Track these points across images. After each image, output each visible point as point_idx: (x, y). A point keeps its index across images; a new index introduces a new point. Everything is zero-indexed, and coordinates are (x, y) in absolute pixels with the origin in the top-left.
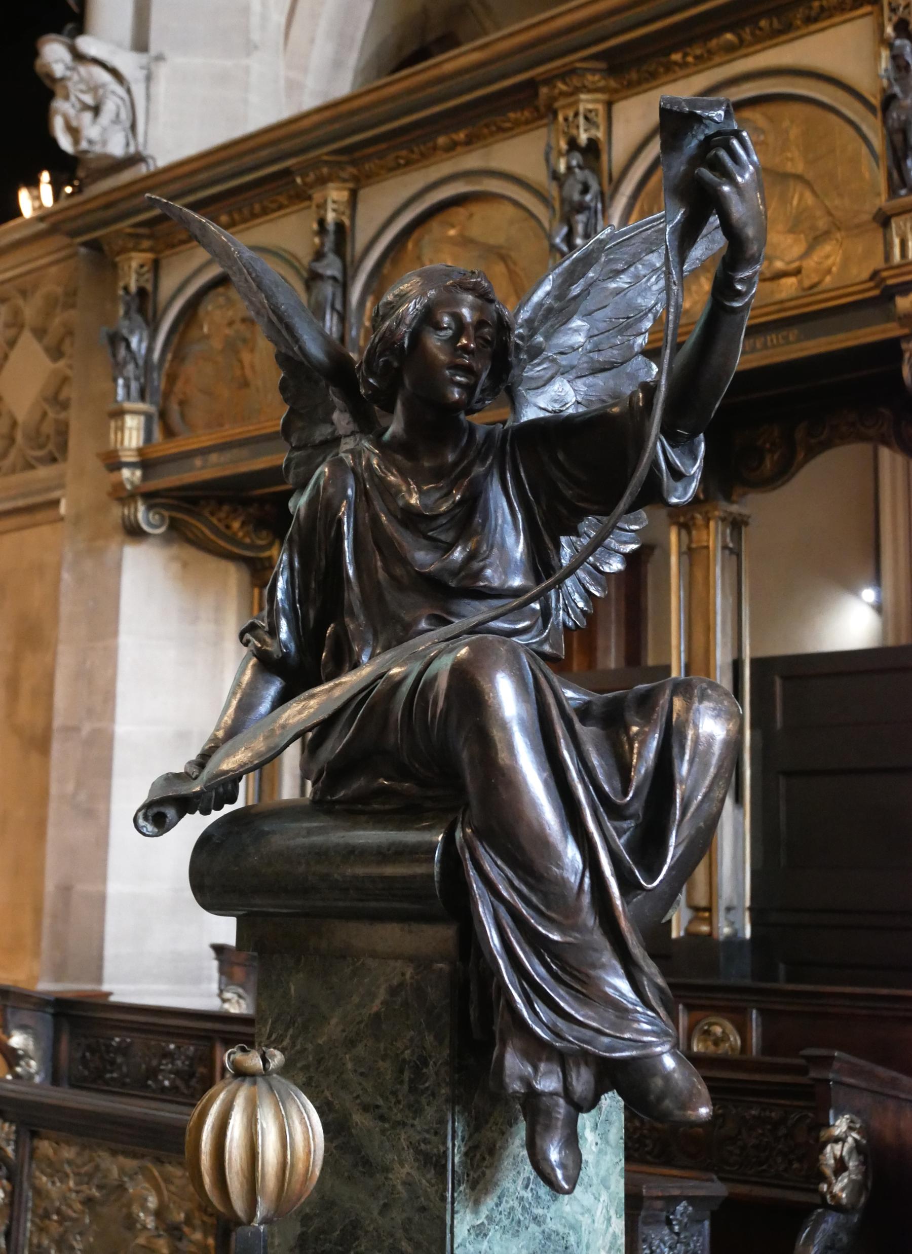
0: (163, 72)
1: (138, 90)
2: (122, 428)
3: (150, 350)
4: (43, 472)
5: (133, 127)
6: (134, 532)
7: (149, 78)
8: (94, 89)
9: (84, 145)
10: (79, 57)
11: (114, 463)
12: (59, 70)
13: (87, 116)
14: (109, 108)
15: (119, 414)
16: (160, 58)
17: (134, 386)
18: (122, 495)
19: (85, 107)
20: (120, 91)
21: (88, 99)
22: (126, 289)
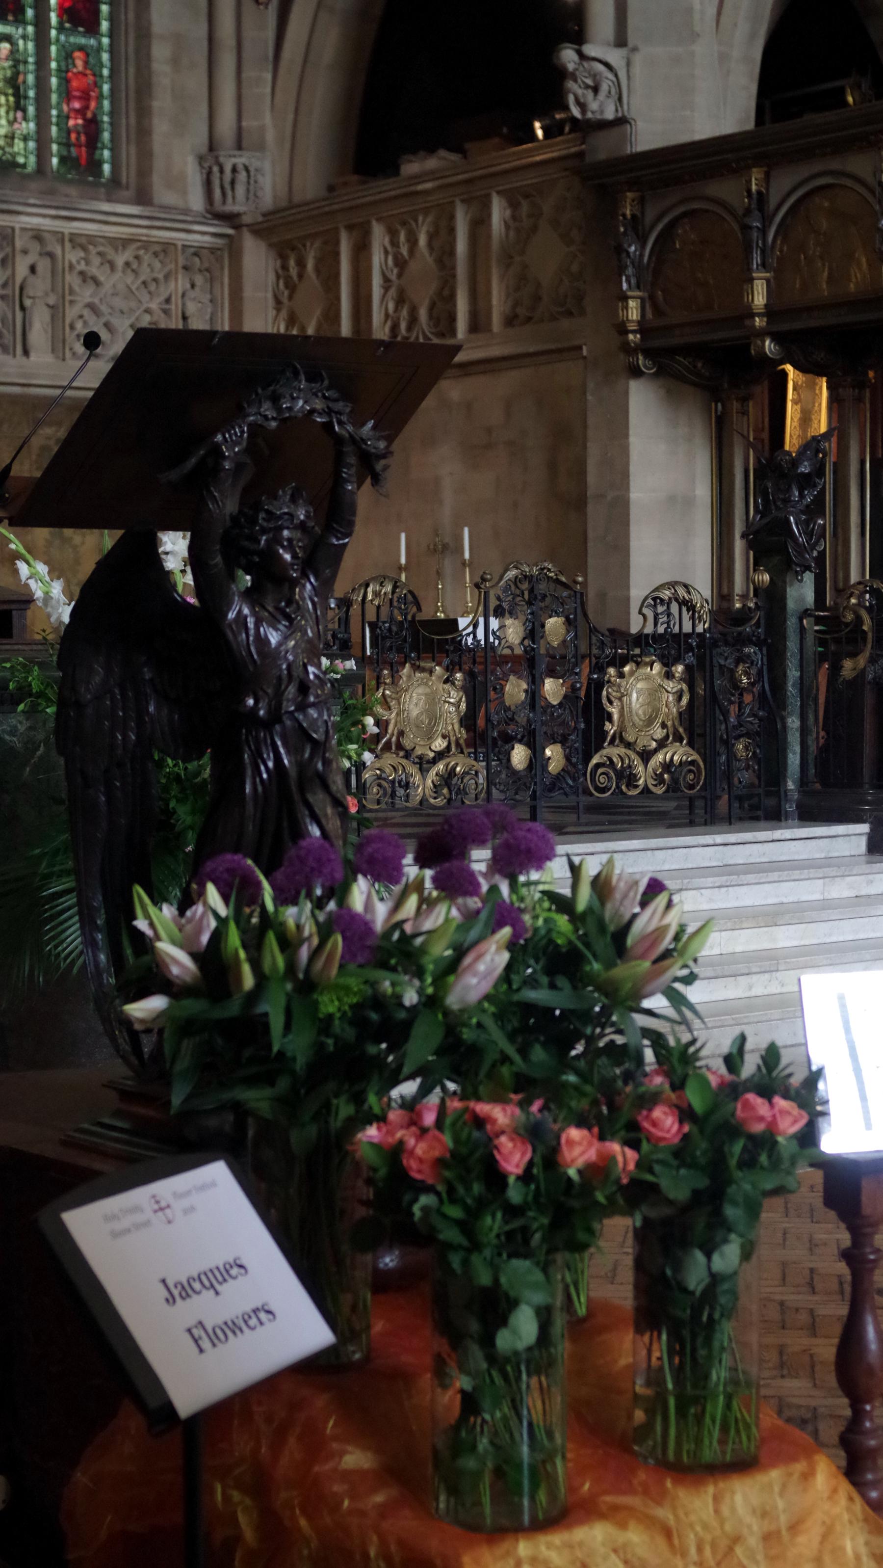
0: (637, 59)
1: (622, 75)
2: (627, 308)
3: (642, 255)
4: (565, 323)
5: (620, 99)
6: (636, 372)
7: (628, 64)
8: (595, 76)
9: (589, 115)
10: (582, 56)
11: (622, 329)
12: (571, 67)
13: (590, 94)
14: (604, 88)
15: (625, 298)
16: (635, 49)
17: (633, 281)
18: (627, 349)
19: (587, 87)
20: (611, 76)
21: (589, 82)
22: (624, 215)
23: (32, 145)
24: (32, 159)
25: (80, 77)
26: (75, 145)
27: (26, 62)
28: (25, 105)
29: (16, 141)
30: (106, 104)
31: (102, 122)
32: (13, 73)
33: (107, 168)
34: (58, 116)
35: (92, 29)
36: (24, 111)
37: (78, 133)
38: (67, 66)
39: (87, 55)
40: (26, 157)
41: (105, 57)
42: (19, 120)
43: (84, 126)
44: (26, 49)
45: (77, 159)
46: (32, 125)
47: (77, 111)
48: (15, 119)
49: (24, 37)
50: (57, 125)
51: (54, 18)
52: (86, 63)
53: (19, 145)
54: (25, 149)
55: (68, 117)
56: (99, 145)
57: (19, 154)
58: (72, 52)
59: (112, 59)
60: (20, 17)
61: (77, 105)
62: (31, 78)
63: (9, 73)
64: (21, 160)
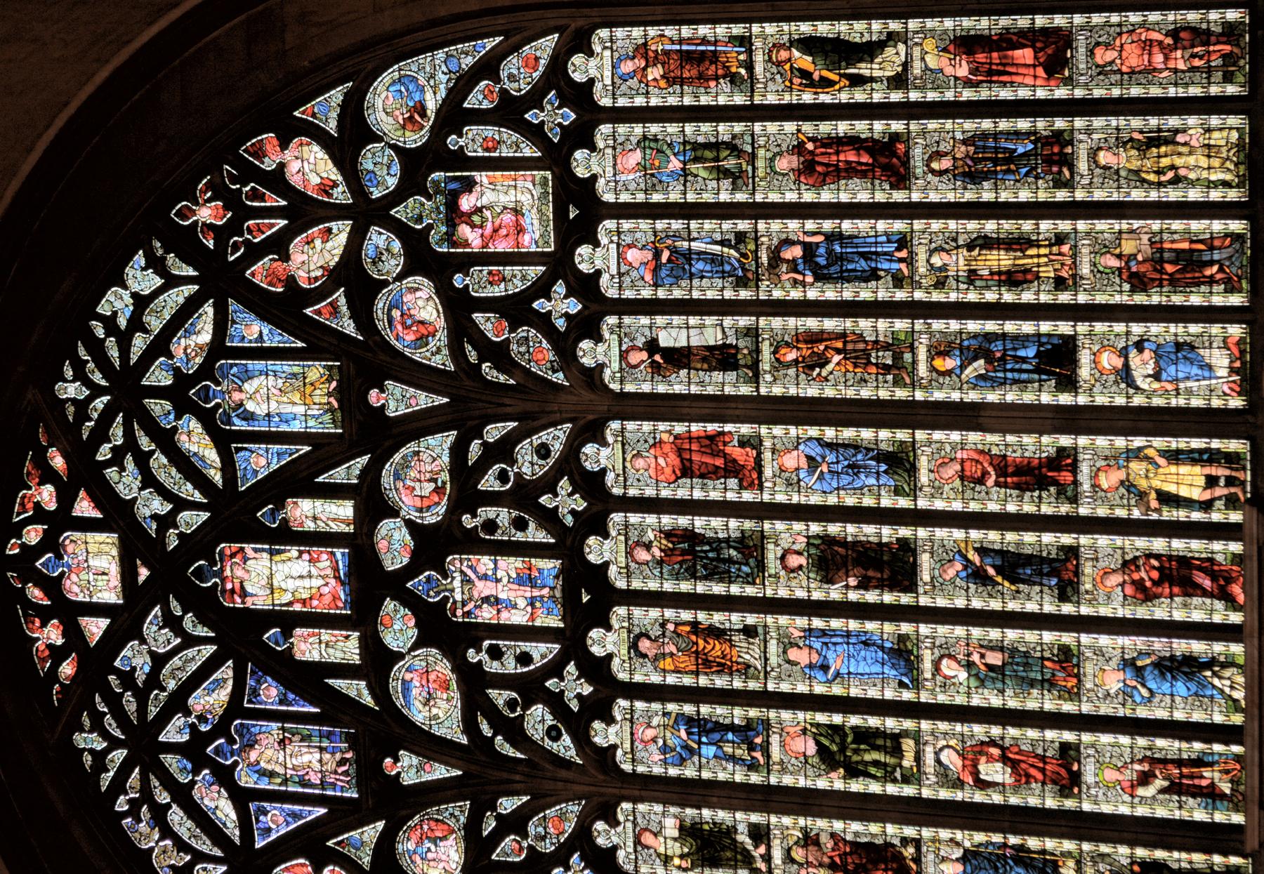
23: (1215, 121)
24: (1233, 120)
25: (1124, 54)
26: (1209, 61)
27: (1118, 129)
28: (1169, 131)
29: (1212, 142)
30: (1154, 17)
31: (1175, 22)
32: (1133, 147)
33: (1232, 15)
34: (1176, 85)
35: (1063, 39)
36: (1177, 131)
37: (1193, 56)
38: (1115, 72)
39: (1098, 44)
40: (1230, 129)
41: (1097, 19)
42: (1188, 139)
43: (1184, 48)
44: (1103, 129)
45: (1224, 57)
46: (1192, 120)
47: (1167, 58)
48: (1185, 144)
49: (1089, 131)
50: (1186, 85)
51: (1061, 93)
52: (1108, 46)
53: (1217, 138)
54: (1221, 129)
55: (1176, 71)
56: (1204, 26)
57: (1227, 138)
58: (1098, 66)
59: (1100, 10)
60: (1066, 136)
61: (1159, 58)
62: (1136, 122)
63: (1134, 152)
64: (1235, 135)
